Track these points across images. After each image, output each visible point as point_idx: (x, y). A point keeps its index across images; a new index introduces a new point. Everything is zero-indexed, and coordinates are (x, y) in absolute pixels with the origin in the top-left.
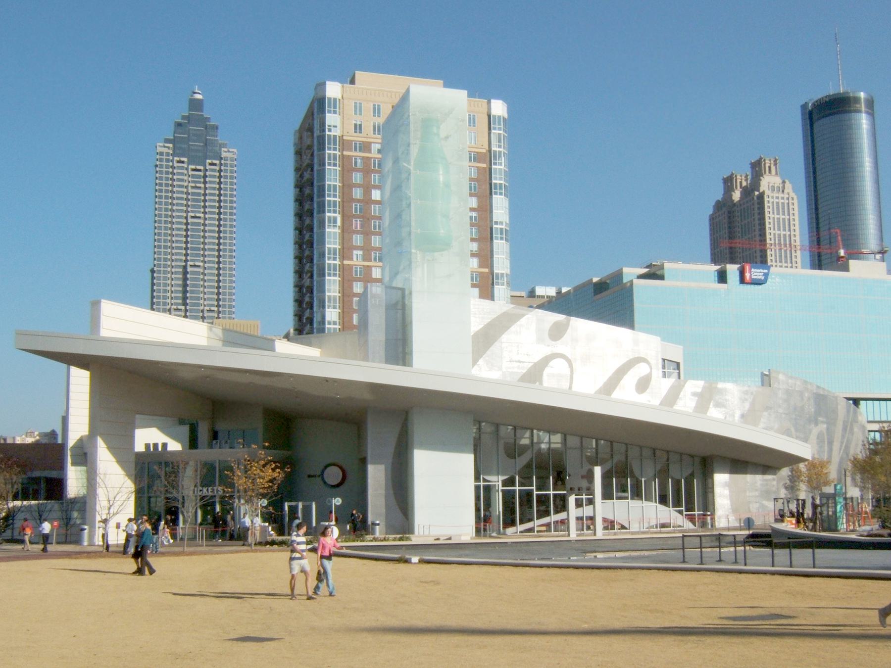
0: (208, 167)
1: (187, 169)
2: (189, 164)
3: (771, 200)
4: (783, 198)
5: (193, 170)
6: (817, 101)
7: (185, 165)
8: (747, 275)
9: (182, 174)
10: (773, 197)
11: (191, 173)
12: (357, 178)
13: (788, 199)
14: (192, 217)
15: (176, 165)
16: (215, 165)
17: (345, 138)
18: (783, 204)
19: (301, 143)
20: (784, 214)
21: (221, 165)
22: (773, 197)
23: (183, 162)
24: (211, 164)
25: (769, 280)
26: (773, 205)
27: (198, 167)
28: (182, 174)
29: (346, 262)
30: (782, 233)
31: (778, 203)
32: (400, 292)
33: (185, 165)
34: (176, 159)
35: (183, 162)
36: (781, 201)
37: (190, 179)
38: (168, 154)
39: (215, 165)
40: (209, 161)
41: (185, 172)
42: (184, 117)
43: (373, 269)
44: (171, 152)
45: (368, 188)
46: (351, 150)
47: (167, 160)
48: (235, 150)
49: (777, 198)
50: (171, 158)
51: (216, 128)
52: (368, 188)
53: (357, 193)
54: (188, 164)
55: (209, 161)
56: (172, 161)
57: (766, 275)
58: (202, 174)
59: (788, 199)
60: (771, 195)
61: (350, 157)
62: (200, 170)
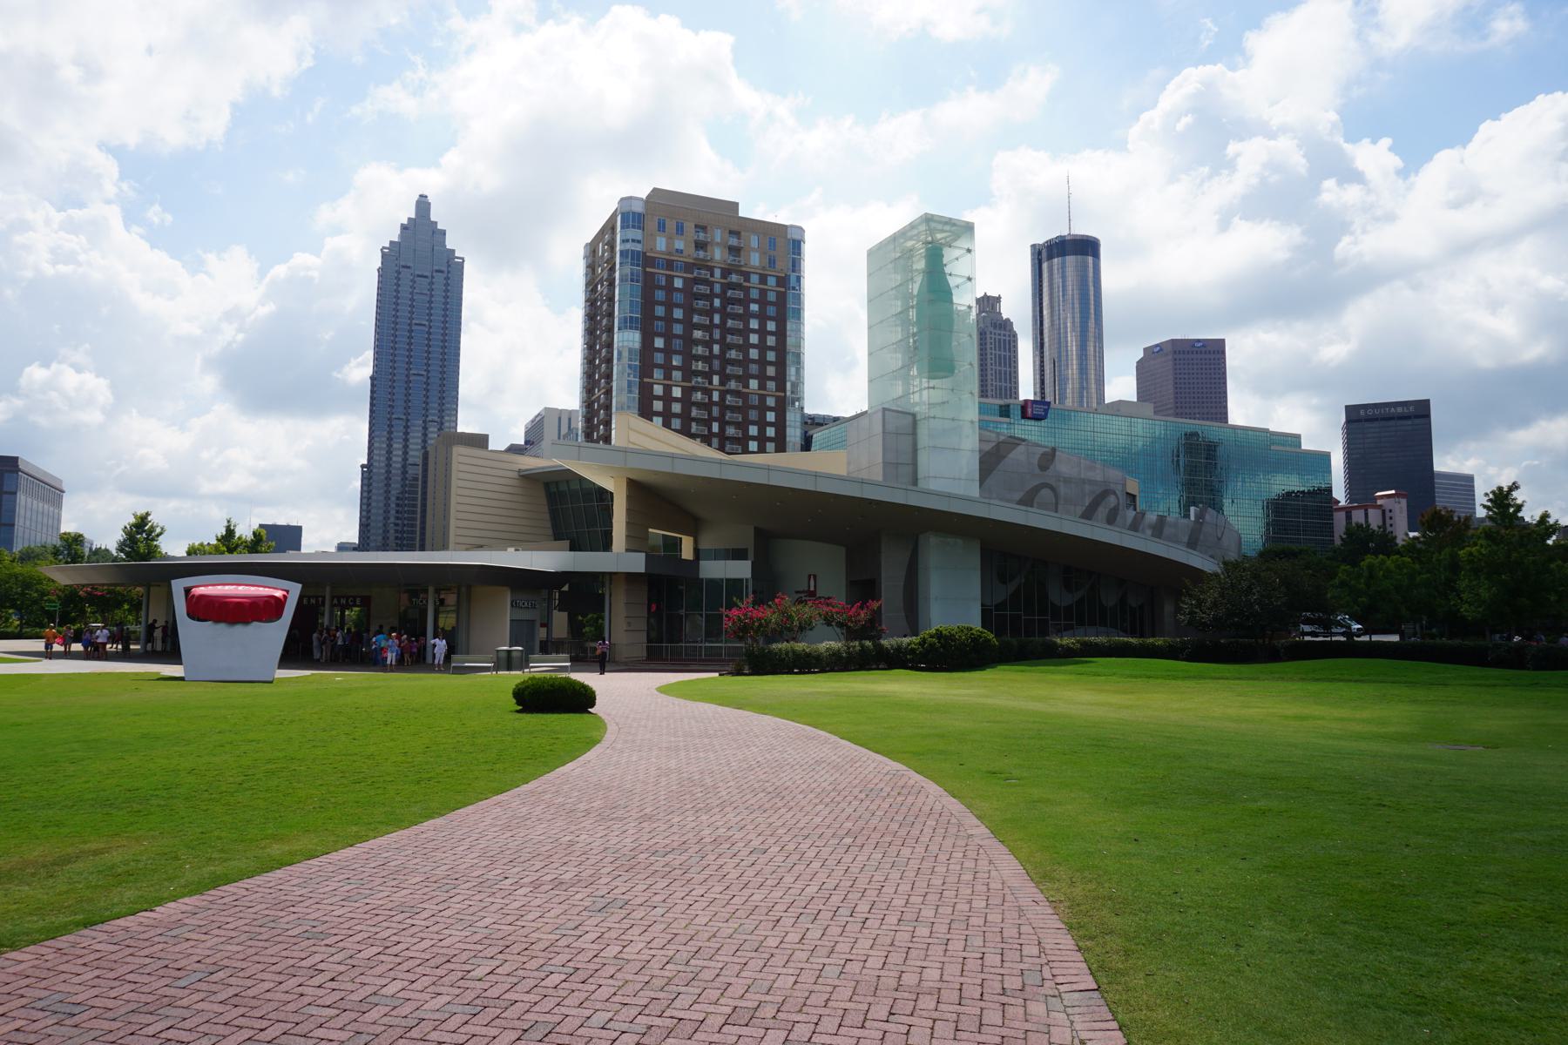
3: (993, 336)
4: (1005, 335)
6: (1047, 242)
8: (1029, 410)
10: (995, 334)
12: (660, 295)
13: (1009, 336)
17: (648, 254)
18: (1005, 340)
19: (594, 256)
20: (1005, 351)
22: (995, 334)
25: (1049, 415)
26: (995, 342)
29: (646, 380)
30: (1003, 369)
31: (1000, 340)
32: (910, 418)
36: (1002, 338)
42: (409, 219)
43: (674, 388)
46: (653, 267)
49: (1000, 335)
51: (444, 233)
53: (660, 311)
55: (436, 268)
57: (1046, 411)
58: (428, 280)
59: (1009, 336)
60: (993, 331)
61: (653, 274)
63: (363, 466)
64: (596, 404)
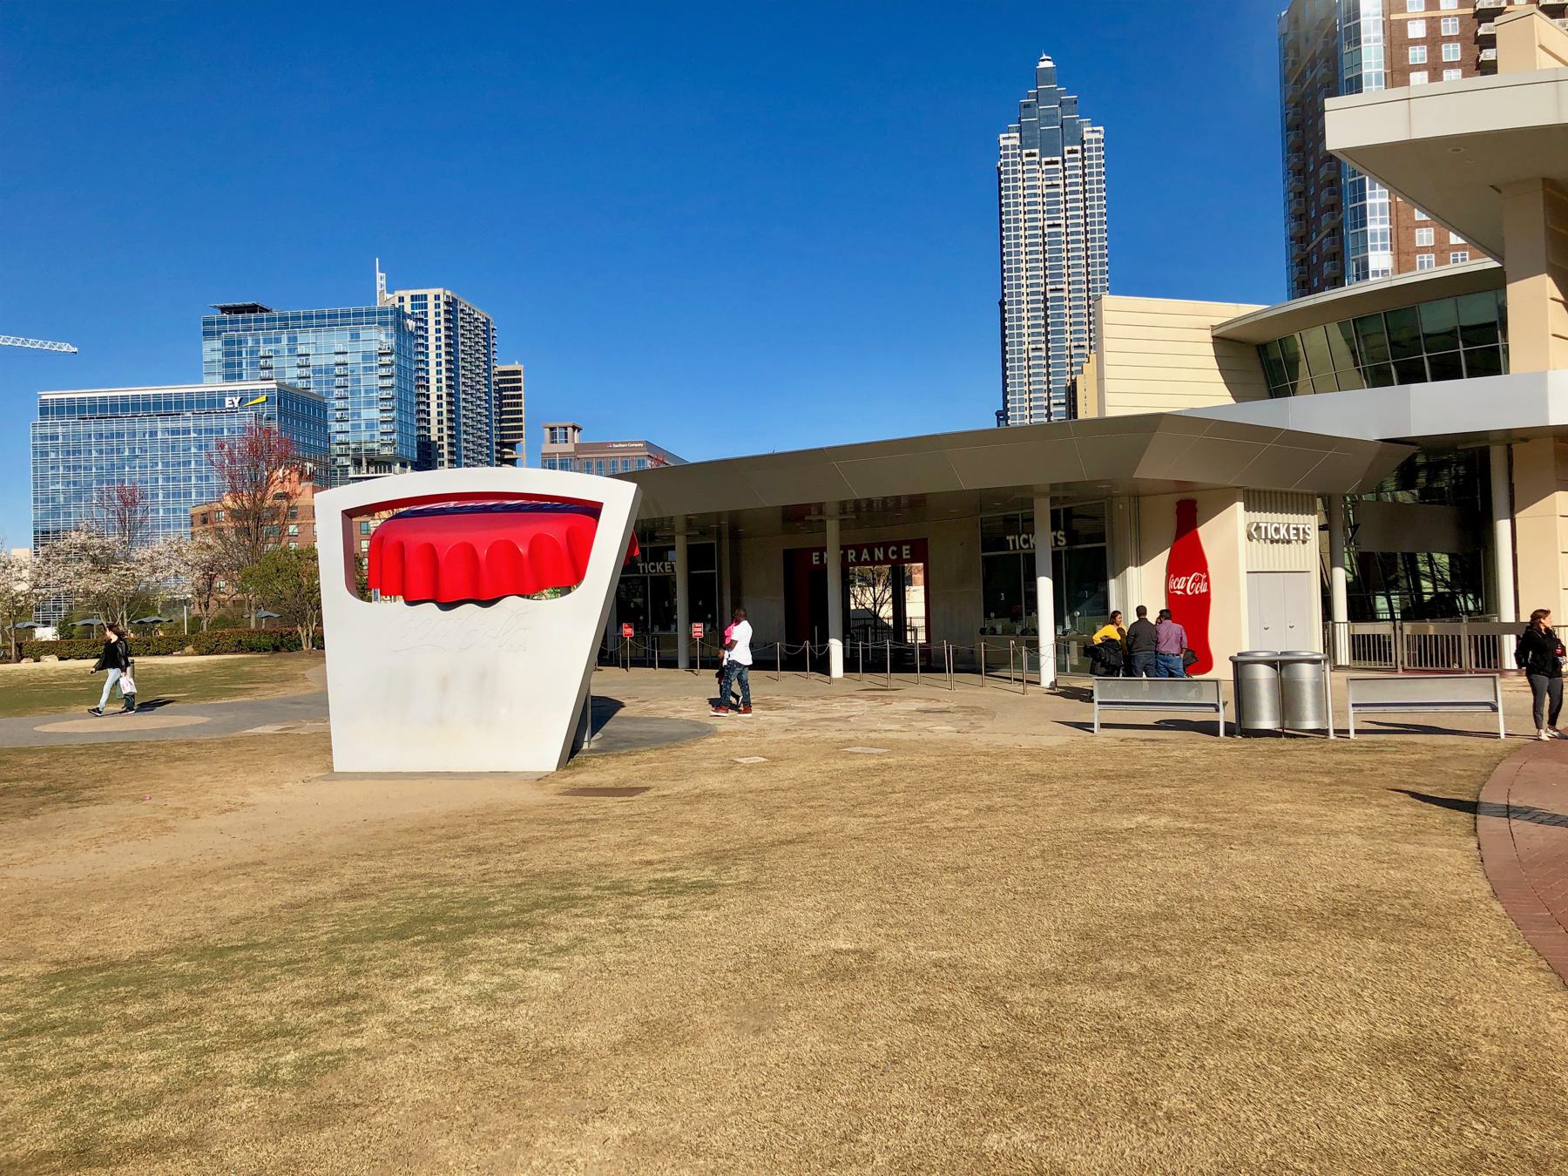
0: (1067, 157)
1: (1040, 163)
2: (1042, 156)
5: (1047, 163)
7: (1037, 159)
9: (1034, 171)
11: (1044, 167)
14: (1049, 226)
15: (1025, 159)
16: (1076, 152)
21: (1083, 150)
23: (1033, 155)
24: (1070, 152)
27: (1054, 159)
28: (1034, 171)
33: (1037, 159)
34: (1025, 152)
35: (1033, 155)
37: (1044, 176)
38: (1014, 147)
39: (1076, 152)
40: (1066, 148)
41: (1038, 167)
44: (1018, 143)
45: (1435, 69)
47: (1014, 156)
48: (1101, 128)
50: (1018, 151)
52: (1435, 69)
54: (1042, 156)
55: (1067, 148)
56: (1020, 155)
58: (1060, 166)
62: (1057, 162)
63: (998, 413)
64: (1315, 258)
